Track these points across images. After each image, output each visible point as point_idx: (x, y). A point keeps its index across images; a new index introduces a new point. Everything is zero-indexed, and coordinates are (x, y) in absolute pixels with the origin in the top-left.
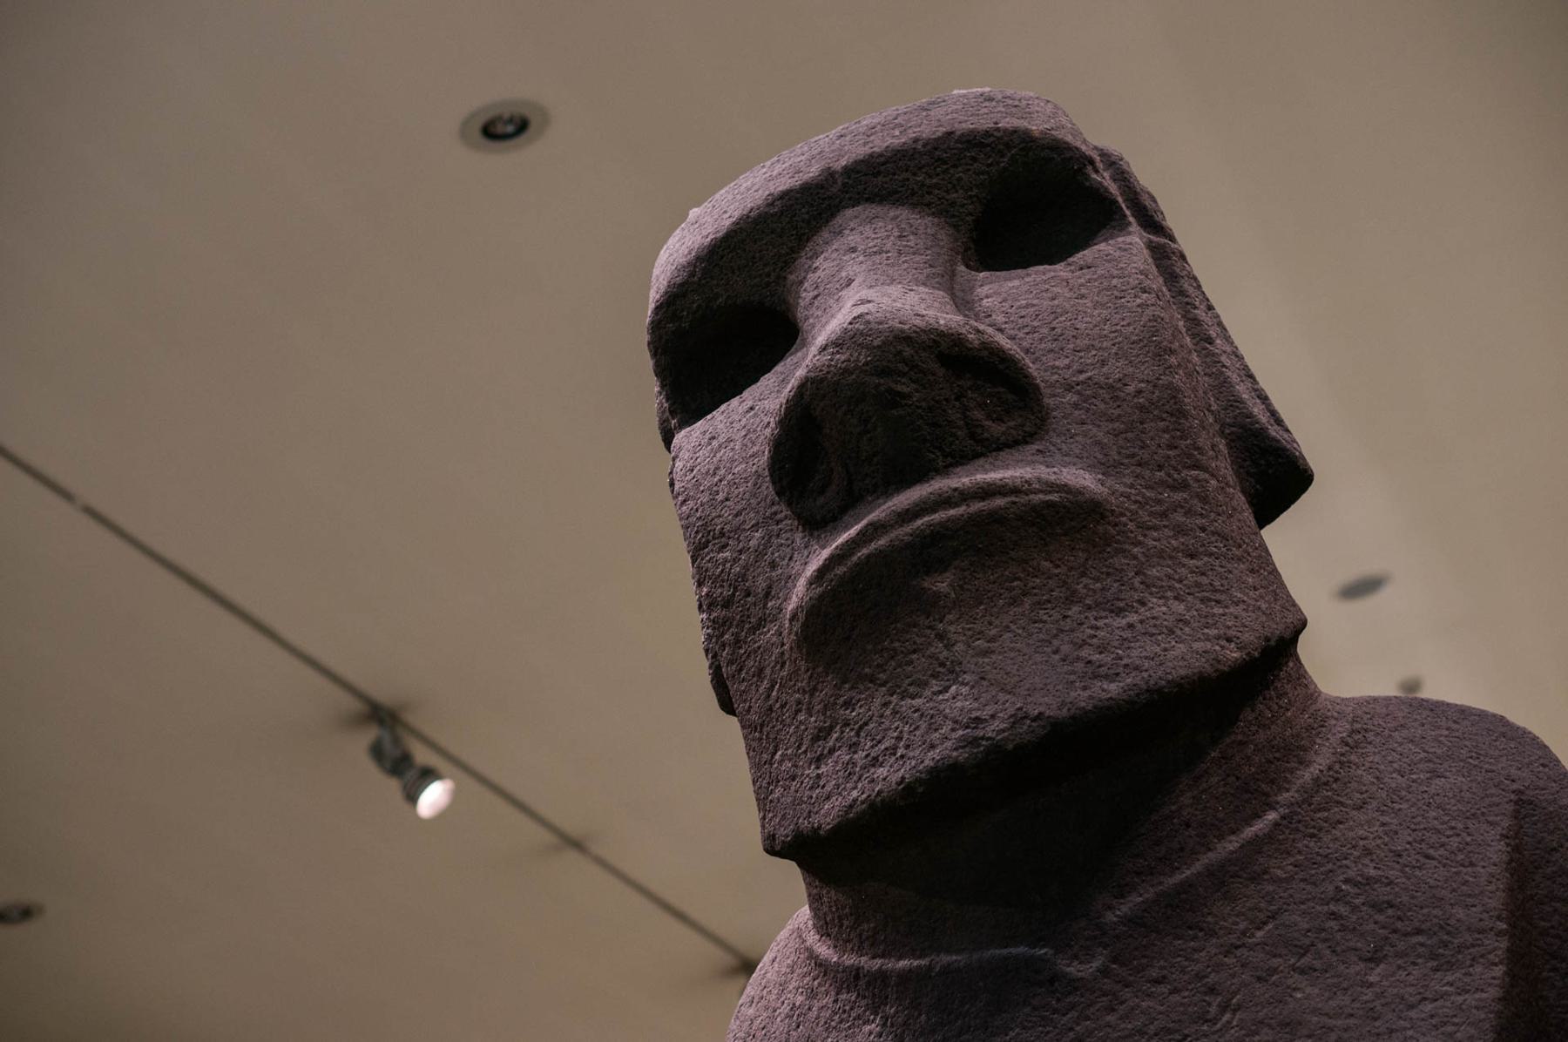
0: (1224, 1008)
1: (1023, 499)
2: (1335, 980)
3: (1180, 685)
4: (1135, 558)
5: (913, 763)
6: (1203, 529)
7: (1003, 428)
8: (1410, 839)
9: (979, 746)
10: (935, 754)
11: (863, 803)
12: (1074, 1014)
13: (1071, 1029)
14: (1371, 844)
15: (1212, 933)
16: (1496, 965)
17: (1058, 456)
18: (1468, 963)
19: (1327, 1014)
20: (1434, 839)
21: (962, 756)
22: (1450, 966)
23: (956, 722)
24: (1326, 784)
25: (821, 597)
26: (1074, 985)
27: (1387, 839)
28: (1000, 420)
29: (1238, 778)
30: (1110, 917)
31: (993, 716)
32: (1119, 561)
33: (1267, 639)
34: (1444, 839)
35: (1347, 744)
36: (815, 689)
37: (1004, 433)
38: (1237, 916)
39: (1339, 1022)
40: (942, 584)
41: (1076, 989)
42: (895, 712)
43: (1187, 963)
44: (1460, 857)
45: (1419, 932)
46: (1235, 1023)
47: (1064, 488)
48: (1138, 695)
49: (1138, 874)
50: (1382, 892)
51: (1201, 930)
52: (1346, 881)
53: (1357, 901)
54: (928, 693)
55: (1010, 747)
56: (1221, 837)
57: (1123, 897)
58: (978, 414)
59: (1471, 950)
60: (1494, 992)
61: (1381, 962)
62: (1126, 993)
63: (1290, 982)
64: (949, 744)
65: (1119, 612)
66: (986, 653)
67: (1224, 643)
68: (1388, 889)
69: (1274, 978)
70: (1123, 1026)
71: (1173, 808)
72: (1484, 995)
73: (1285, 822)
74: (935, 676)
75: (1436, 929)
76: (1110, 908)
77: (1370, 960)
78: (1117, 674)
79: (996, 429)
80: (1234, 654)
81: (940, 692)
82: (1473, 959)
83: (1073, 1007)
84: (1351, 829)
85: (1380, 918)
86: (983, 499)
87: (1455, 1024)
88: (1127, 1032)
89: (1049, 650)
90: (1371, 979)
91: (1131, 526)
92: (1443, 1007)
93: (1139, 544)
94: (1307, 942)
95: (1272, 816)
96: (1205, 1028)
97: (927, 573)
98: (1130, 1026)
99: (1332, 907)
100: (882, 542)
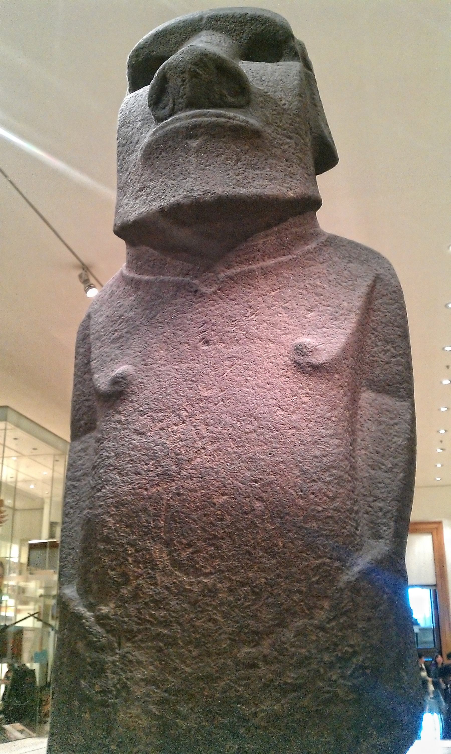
0: (252, 314)
1: (232, 121)
2: (295, 313)
3: (268, 197)
4: (267, 154)
5: (166, 201)
6: (293, 154)
7: (233, 100)
8: (335, 277)
9: (191, 198)
10: (175, 199)
11: (145, 212)
12: (200, 304)
13: (197, 309)
14: (321, 275)
15: (256, 288)
16: (353, 323)
17: (250, 115)
18: (343, 320)
19: (288, 324)
20: (344, 279)
21: (182, 201)
22: (336, 319)
23: (185, 189)
24: (312, 252)
25: (152, 141)
26: (203, 295)
27: (327, 275)
28: (233, 97)
29: (281, 241)
30: (222, 275)
31: (198, 190)
32: (260, 154)
33: (305, 195)
34: (347, 280)
35: (323, 244)
36: (142, 175)
37: (233, 102)
38: (267, 285)
39: (291, 327)
40: (194, 144)
41: (203, 296)
42: (166, 184)
43: (245, 296)
44: (351, 287)
45: (329, 306)
46: (255, 319)
47: (247, 122)
48: (252, 195)
49: (236, 262)
50: (319, 290)
51: (253, 286)
52: (309, 284)
53: (310, 291)
54: (178, 179)
55: (201, 201)
56: (269, 258)
57: (229, 269)
58: (225, 92)
59: (346, 316)
60: (349, 331)
61: (313, 312)
62: (220, 301)
63: (278, 310)
64: (180, 196)
65: (254, 169)
66: (203, 170)
67: (289, 190)
68: (323, 290)
69: (273, 308)
70: (216, 312)
71: (256, 243)
72: (345, 331)
73: (294, 260)
74: (182, 174)
75: (335, 306)
76: (223, 271)
77: (309, 310)
78: (247, 187)
79: (230, 100)
80: (291, 194)
81: (183, 180)
82: (345, 319)
83: (200, 302)
84: (316, 269)
85: (317, 298)
86: (217, 118)
87: (332, 337)
88: (216, 314)
89: (225, 174)
90: (309, 316)
91: (268, 144)
92: (330, 331)
93: (269, 150)
94: (289, 299)
95: (290, 257)
96: (244, 318)
97: (191, 138)
98: (218, 312)
99: (301, 291)
100: (178, 124)
